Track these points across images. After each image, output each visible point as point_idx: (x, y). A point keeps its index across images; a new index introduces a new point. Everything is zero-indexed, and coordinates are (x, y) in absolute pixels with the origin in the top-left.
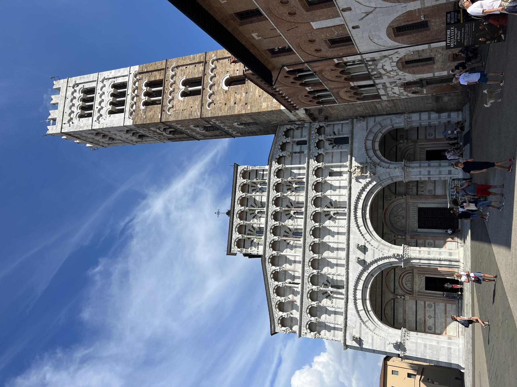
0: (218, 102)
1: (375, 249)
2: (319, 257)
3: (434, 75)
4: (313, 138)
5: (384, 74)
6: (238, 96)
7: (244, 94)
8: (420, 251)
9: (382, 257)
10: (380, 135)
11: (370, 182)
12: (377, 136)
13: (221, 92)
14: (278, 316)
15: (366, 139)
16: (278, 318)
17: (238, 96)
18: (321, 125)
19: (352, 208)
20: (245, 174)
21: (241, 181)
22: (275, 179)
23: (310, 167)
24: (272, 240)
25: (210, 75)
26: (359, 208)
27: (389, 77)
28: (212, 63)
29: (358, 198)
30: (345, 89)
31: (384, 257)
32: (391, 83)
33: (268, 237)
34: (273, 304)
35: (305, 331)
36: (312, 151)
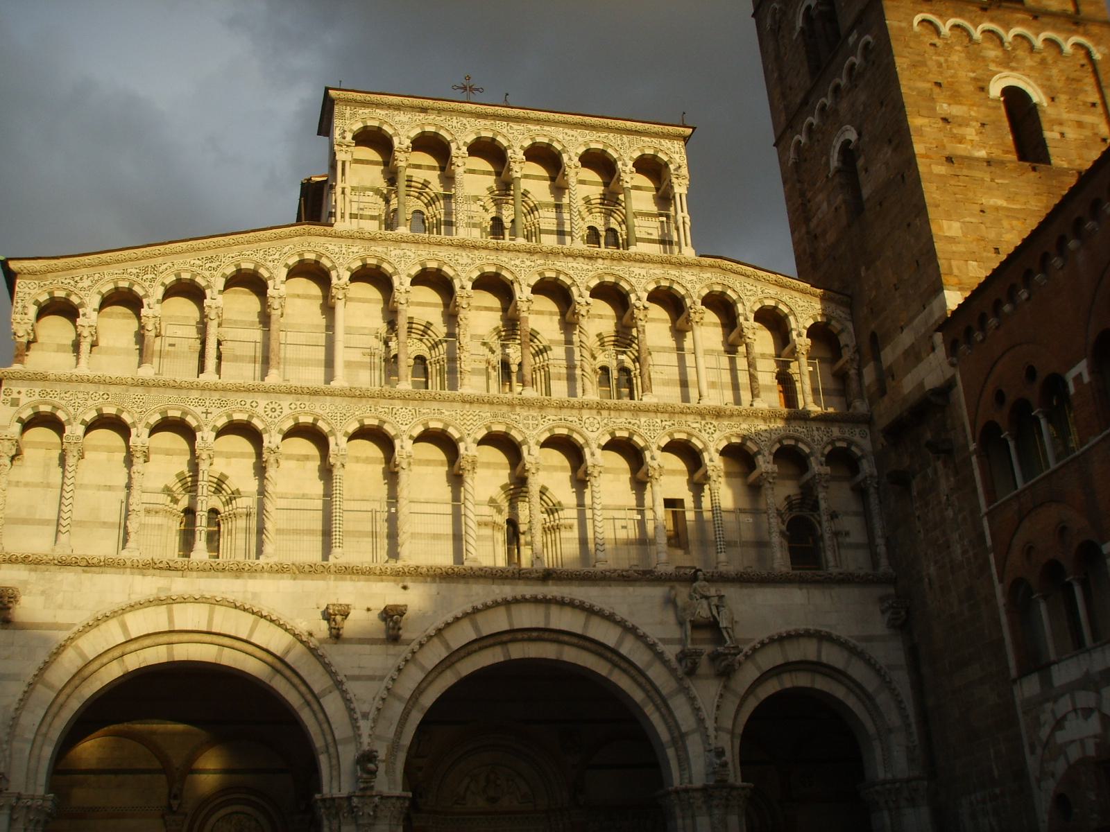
0: (942, 59)
1: (384, 684)
4: (816, 433)
6: (974, 133)
7: (982, 153)
10: (839, 692)
12: (832, 678)
14: (82, 289)
15: (822, 637)
17: (971, 132)
18: (867, 467)
19: (552, 590)
22: (644, 281)
26: (547, 617)
28: (1078, 46)
29: (590, 611)
31: (356, 720)
33: (409, 253)
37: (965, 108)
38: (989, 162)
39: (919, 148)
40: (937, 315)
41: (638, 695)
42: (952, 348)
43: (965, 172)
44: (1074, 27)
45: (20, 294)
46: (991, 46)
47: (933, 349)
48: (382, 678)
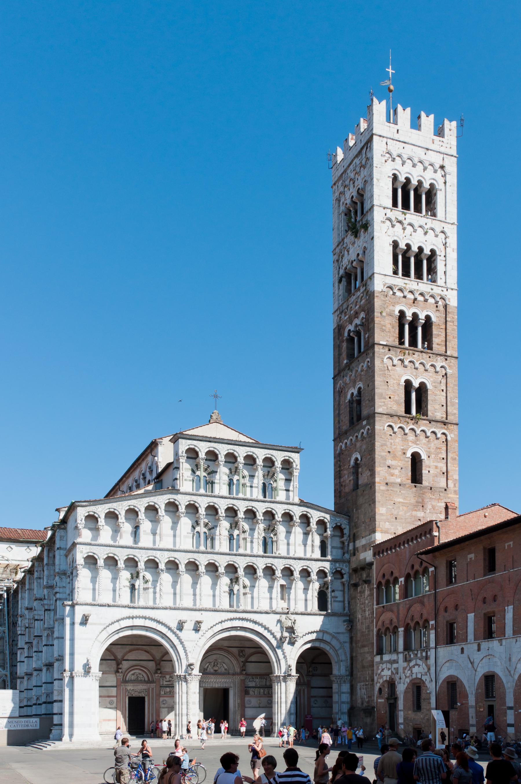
0: (392, 441)
3: (401, 710)
5: (409, 665)
7: (399, 480)
8: (195, 693)
11: (274, 637)
13: (405, 446)
17: (396, 472)
20: (287, 465)
21: (279, 457)
25: (429, 430)
27: (404, 669)
29: (255, 623)
30: (395, 620)
32: (397, 669)
37: (397, 462)
38: (400, 485)
39: (377, 480)
40: (373, 540)
41: (267, 647)
42: (374, 555)
43: (391, 488)
44: (444, 426)
46: (412, 435)
47: (370, 550)
48: (195, 641)
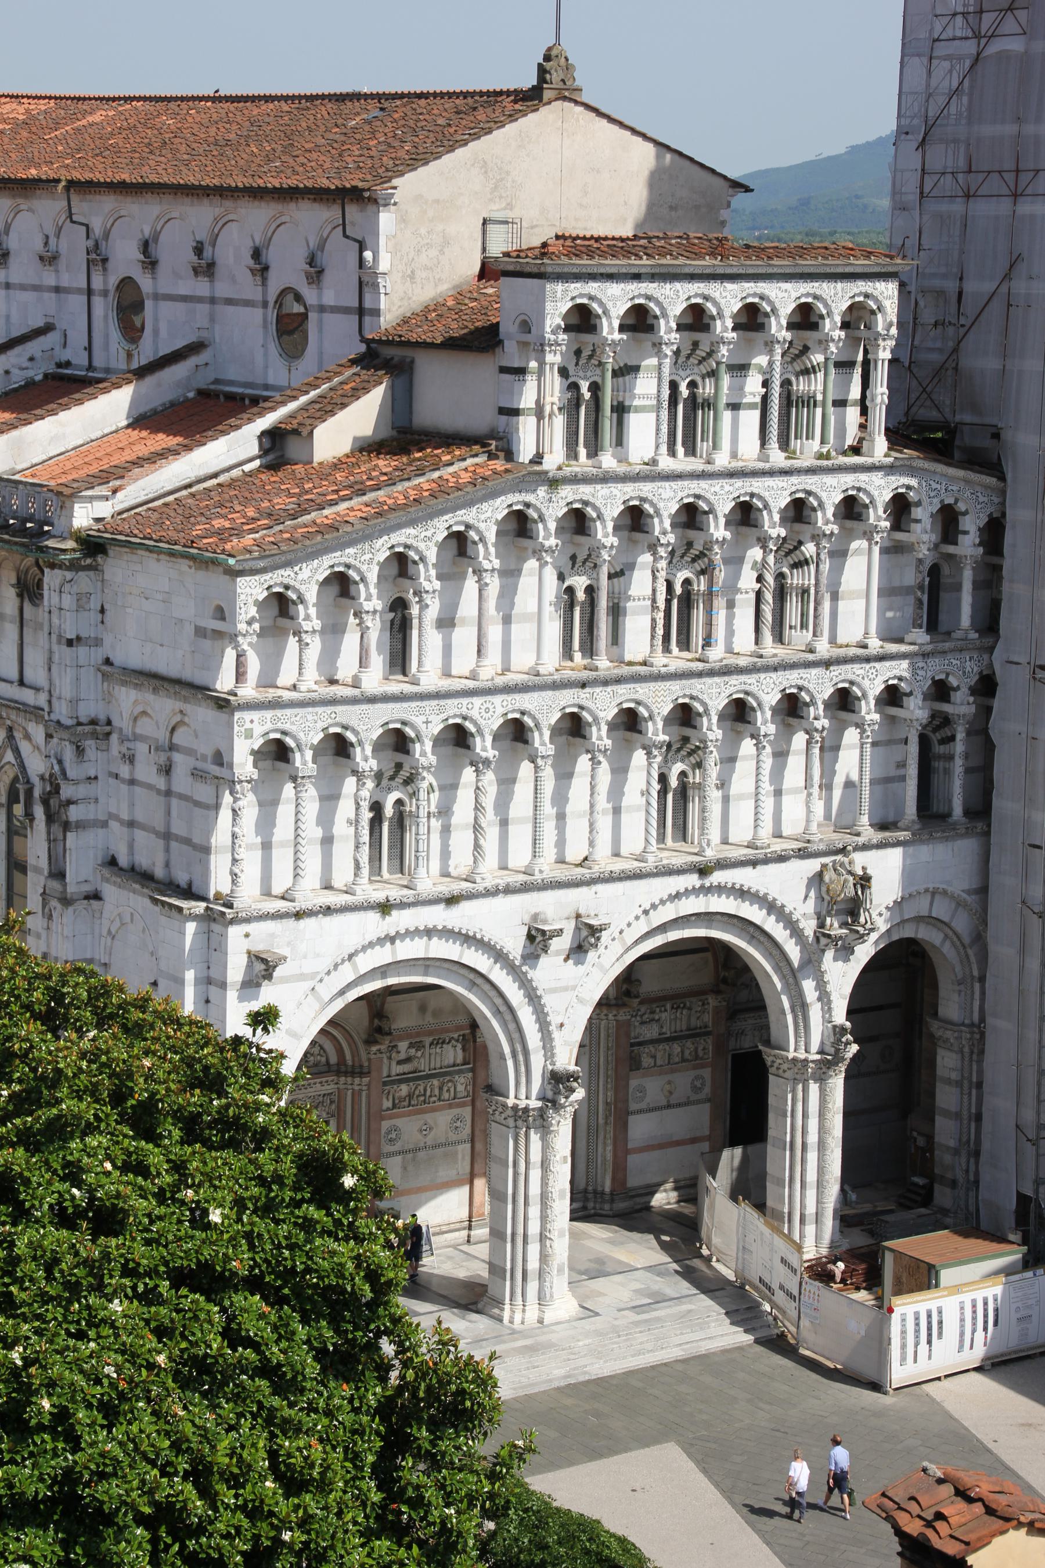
2: (543, 757)
9: (549, 1024)
11: (796, 932)
14: (303, 582)
16: (298, 586)
23: (868, 666)
24: (603, 510)
33: (615, 492)
34: (351, 551)
35: (258, 730)
36: (921, 665)
45: (243, 597)
